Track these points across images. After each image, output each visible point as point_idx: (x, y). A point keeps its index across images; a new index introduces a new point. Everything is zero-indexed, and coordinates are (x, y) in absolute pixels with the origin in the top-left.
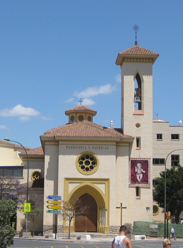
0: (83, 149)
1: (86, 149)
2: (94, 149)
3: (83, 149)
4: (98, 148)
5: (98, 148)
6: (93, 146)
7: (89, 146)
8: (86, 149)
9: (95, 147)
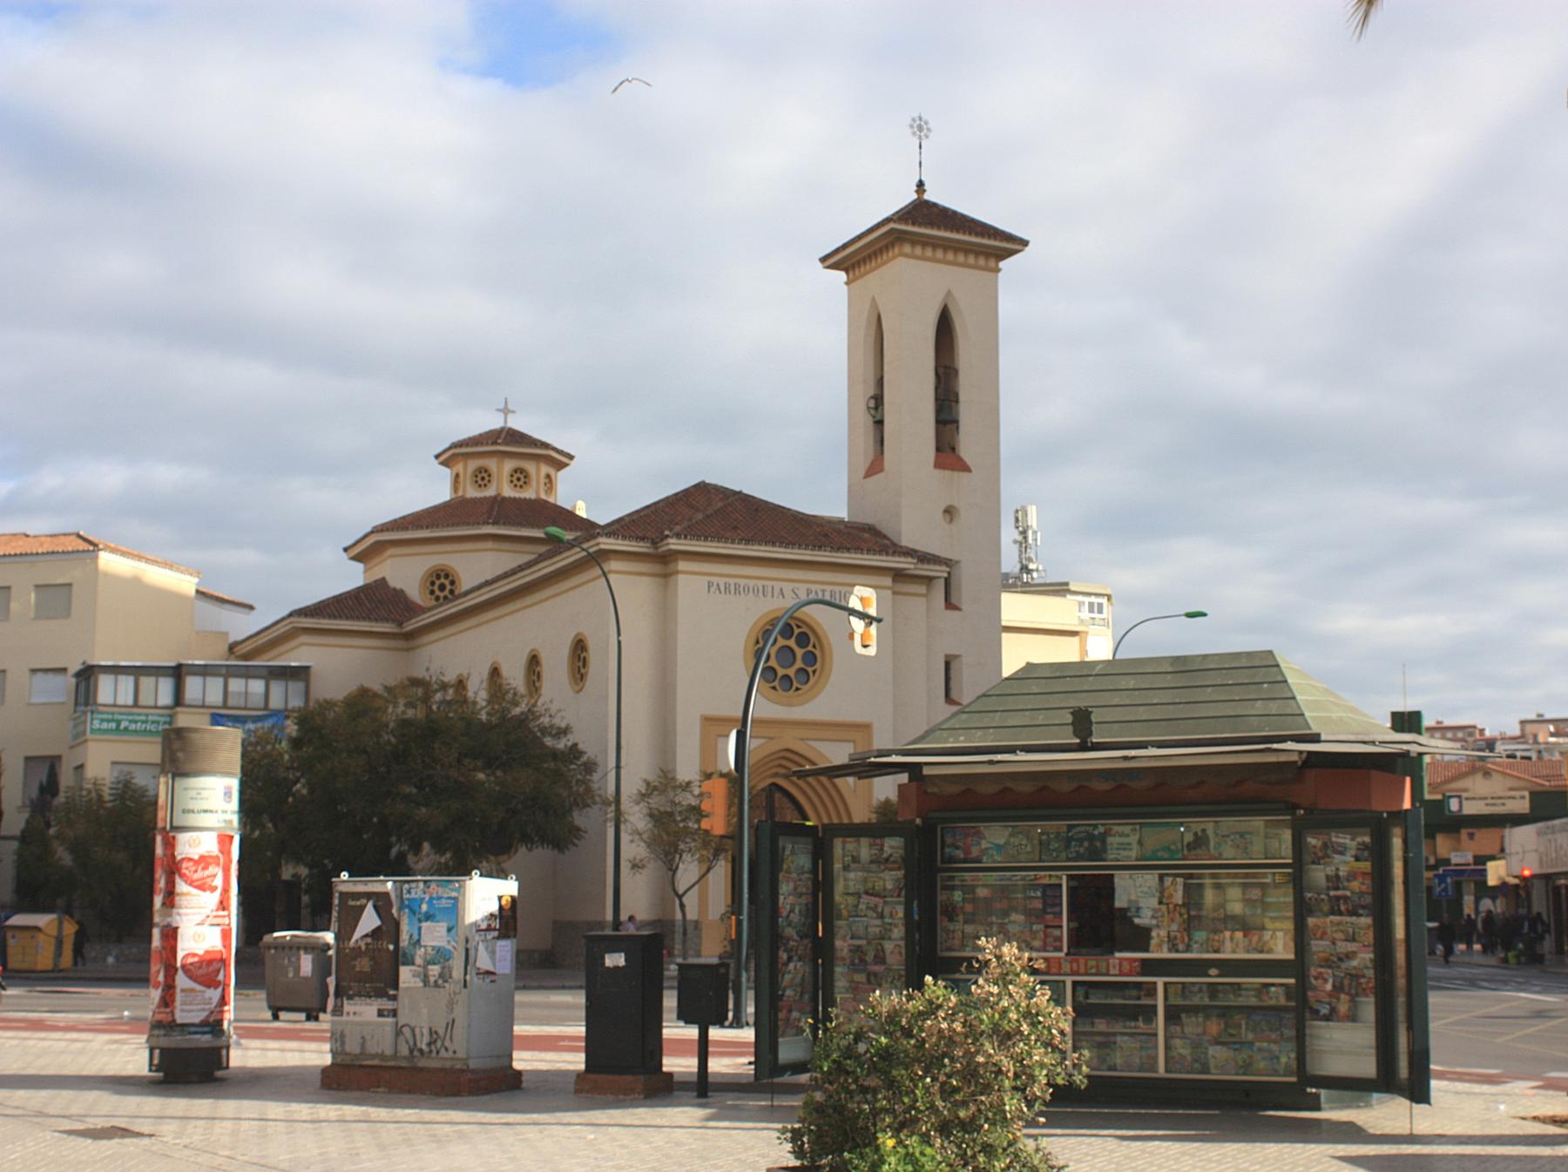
0: (773, 596)
1: (783, 597)
2: (778, 597)
3: (773, 596)
4: (777, 591)
5: (777, 591)
6: (808, 586)
7: (796, 585)
8: (783, 597)
9: (718, 585)
